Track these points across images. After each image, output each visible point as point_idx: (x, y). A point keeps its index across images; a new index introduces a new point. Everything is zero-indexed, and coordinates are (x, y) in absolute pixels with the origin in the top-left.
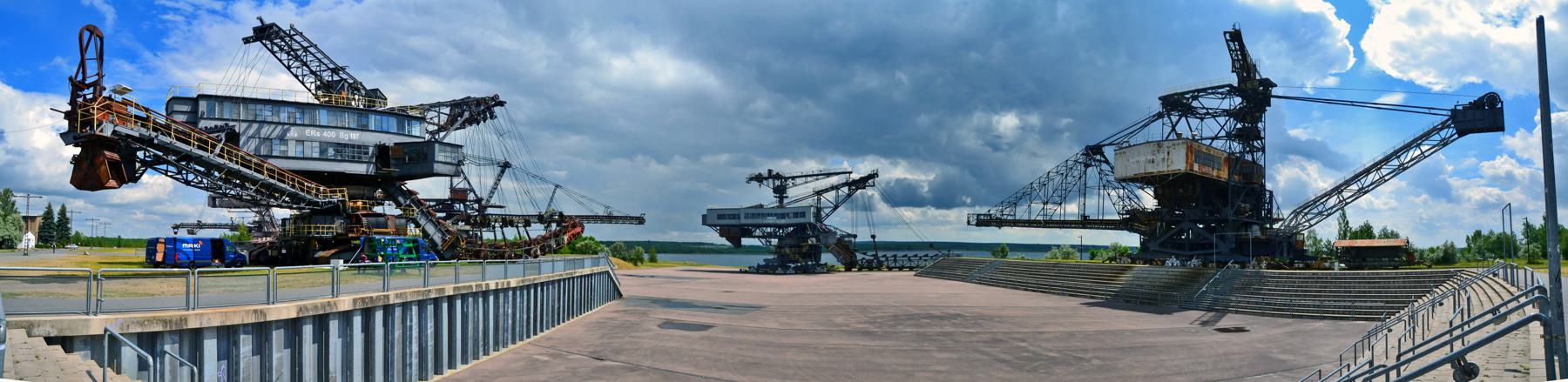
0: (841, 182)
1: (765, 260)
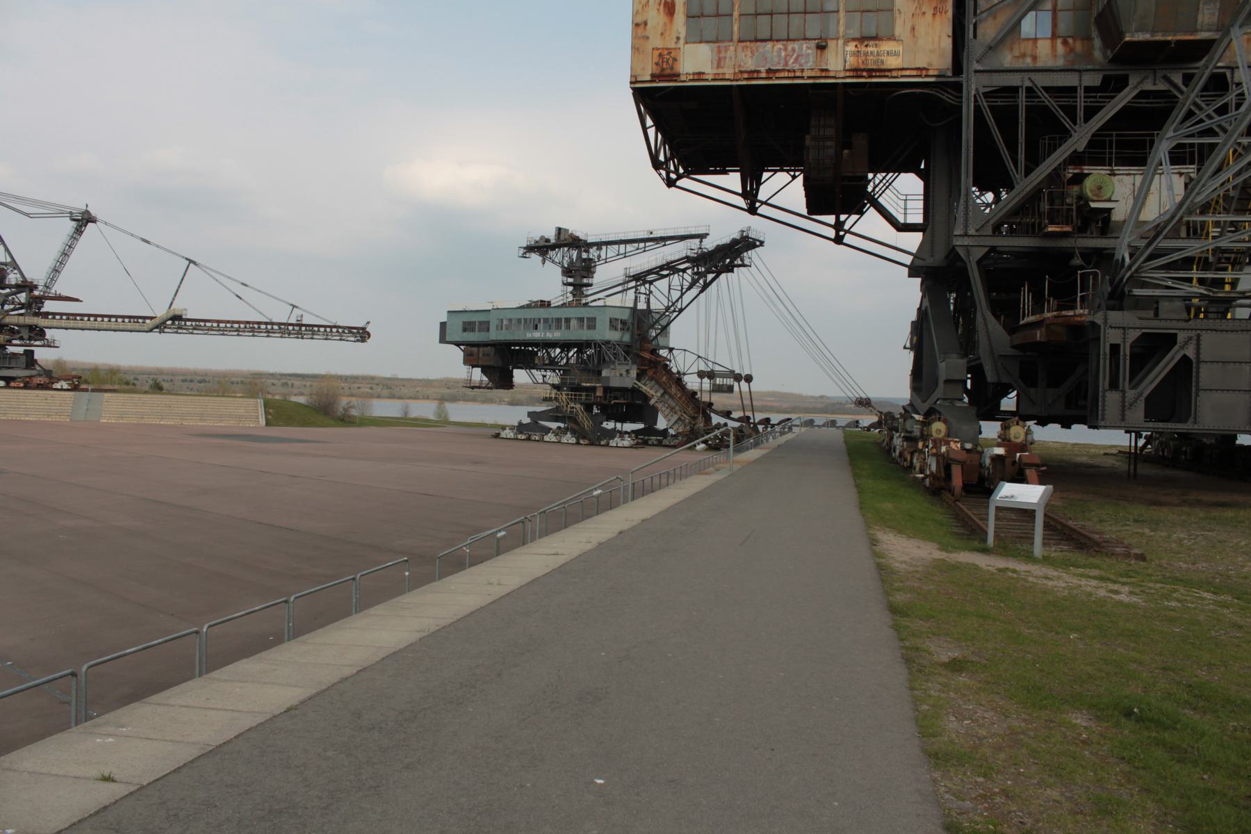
1: (530, 414)
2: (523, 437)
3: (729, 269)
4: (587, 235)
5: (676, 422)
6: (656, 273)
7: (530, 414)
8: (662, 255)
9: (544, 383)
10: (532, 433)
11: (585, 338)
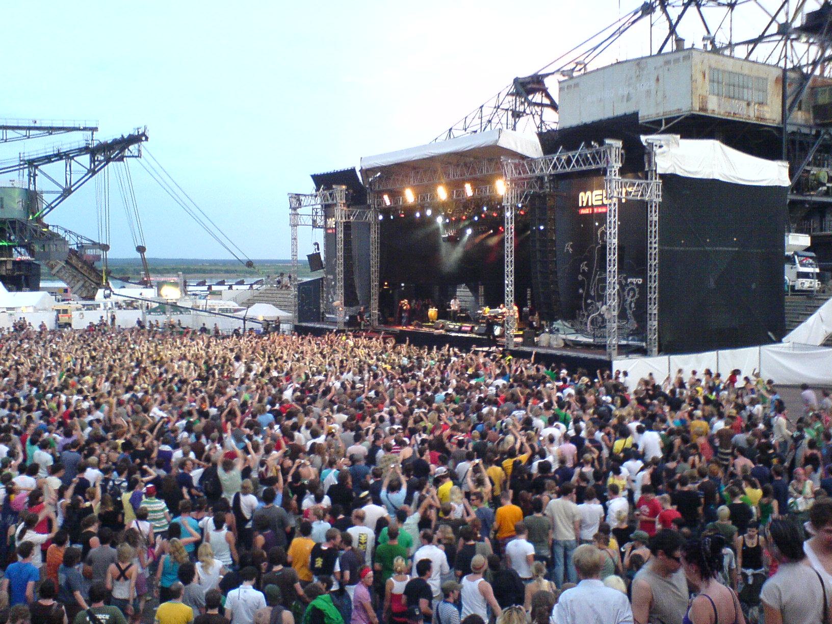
0: (76, 146)
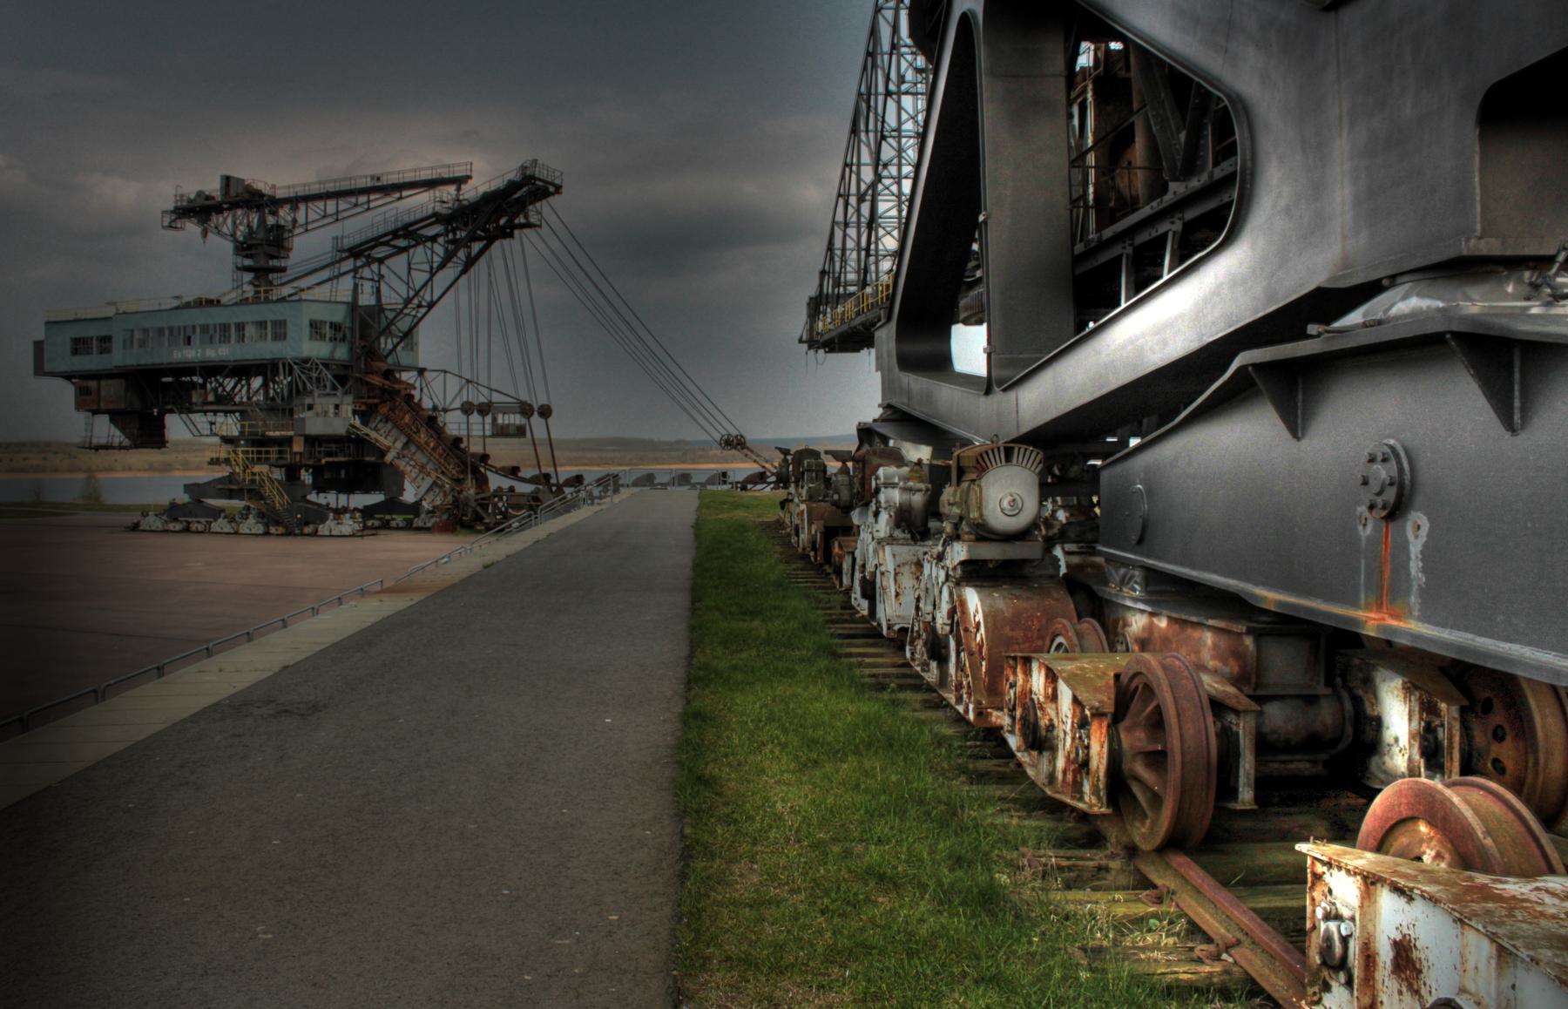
1: (189, 488)
2: (178, 527)
3: (506, 233)
4: (274, 187)
5: (430, 489)
6: (386, 244)
7: (189, 488)
8: (394, 212)
9: (213, 434)
10: (194, 519)
11: (268, 356)
